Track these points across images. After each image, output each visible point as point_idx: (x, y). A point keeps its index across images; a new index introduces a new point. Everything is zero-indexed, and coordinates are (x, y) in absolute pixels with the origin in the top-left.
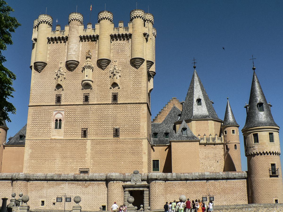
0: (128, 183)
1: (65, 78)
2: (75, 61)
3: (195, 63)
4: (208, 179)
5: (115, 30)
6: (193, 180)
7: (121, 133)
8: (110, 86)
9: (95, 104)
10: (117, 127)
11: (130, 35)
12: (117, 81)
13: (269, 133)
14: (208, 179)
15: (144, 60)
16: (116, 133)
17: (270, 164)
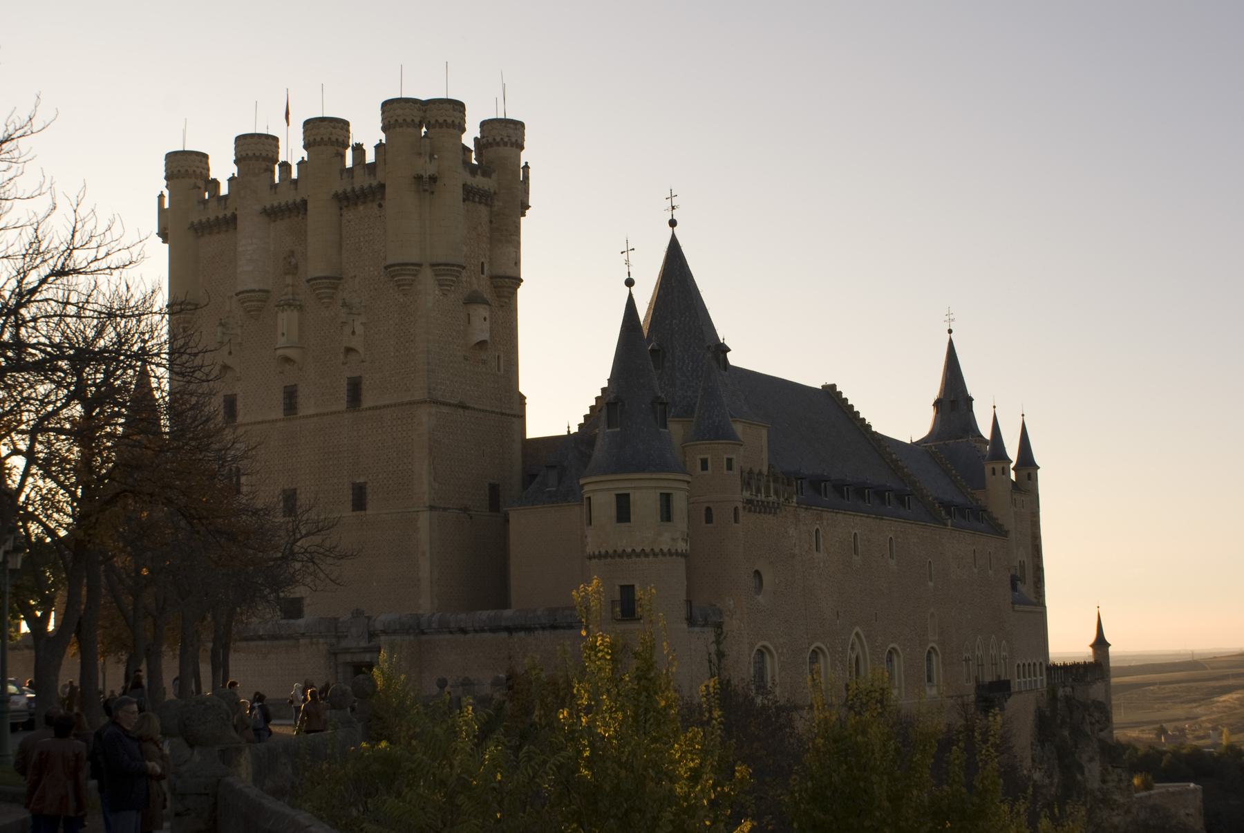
0: (344, 644)
1: (241, 344)
2: (253, 291)
3: (673, 208)
4: (509, 630)
5: (345, 175)
6: (476, 631)
7: (369, 497)
8: (342, 356)
9: (313, 416)
10: (362, 480)
11: (382, 187)
12: (353, 345)
13: (617, 495)
14: (509, 630)
15: (420, 265)
16: (359, 499)
17: (617, 588)
